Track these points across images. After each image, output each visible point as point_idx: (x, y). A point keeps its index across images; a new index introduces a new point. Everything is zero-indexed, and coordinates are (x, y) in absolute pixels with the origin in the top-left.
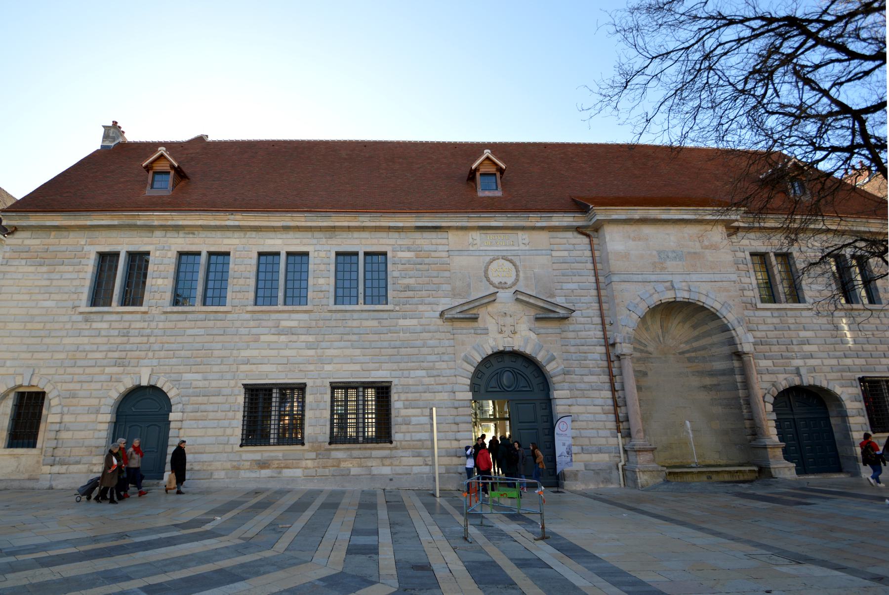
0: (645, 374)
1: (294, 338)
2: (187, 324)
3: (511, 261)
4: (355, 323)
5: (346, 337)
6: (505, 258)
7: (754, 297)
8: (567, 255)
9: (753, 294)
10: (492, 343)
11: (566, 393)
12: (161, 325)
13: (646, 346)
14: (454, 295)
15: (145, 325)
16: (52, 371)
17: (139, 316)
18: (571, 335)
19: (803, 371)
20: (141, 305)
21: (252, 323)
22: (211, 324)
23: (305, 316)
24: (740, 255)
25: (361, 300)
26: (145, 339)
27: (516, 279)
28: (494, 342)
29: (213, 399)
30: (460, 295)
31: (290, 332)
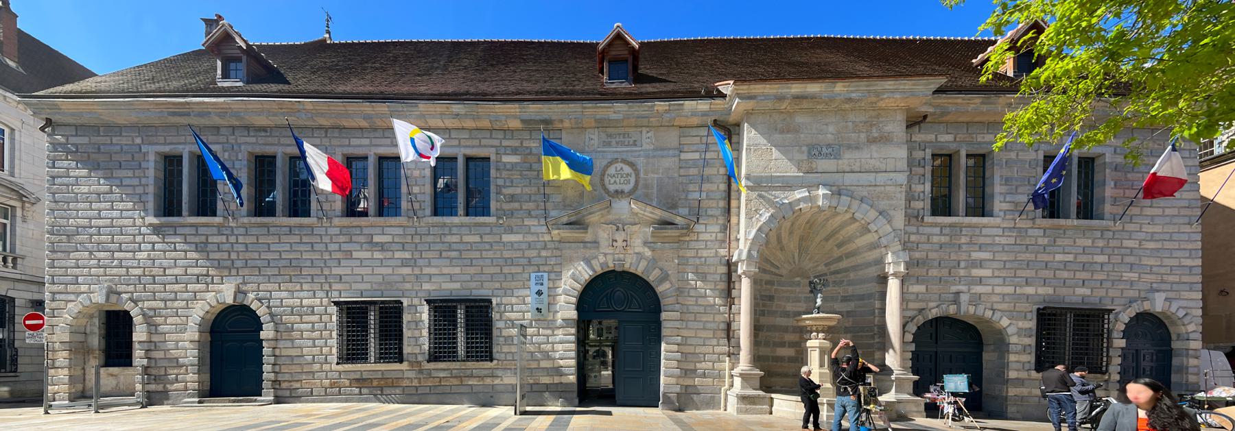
0: (771, 298)
1: (389, 254)
2: (270, 240)
3: (632, 165)
4: (455, 239)
5: (444, 254)
6: (624, 161)
7: (923, 209)
8: (698, 157)
9: (923, 205)
10: (602, 259)
11: (676, 315)
12: (241, 239)
13: (778, 268)
14: (565, 206)
15: (224, 239)
16: (131, 288)
17: (215, 230)
18: (692, 253)
19: (964, 298)
20: (214, 214)
21: (342, 239)
22: (297, 239)
23: (400, 230)
24: (918, 154)
25: (461, 210)
26: (225, 255)
28: (606, 260)
29: (305, 318)
30: (571, 206)
31: (382, 247)
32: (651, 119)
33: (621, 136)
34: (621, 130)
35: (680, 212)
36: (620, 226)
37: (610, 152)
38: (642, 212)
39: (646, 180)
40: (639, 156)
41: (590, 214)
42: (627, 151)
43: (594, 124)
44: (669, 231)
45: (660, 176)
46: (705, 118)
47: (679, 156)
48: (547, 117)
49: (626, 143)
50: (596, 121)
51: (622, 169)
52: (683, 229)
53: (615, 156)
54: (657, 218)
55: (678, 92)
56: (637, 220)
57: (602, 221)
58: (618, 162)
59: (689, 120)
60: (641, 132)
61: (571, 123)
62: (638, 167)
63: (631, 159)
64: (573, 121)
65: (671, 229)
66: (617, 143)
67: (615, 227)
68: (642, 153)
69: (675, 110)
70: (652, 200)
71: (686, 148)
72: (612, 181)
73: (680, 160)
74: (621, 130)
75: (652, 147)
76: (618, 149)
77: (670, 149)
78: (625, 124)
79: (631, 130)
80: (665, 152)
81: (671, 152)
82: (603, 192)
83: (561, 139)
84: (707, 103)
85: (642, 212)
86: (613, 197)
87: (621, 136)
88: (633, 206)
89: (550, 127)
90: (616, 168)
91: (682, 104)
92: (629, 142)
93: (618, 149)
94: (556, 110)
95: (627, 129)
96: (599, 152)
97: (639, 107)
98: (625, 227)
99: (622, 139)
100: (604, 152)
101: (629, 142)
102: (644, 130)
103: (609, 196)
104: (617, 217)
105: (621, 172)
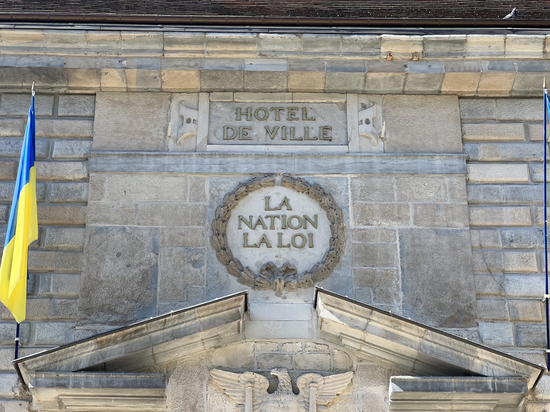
8: (526, 179)
27: (328, 255)
30: (111, 311)
32: (372, 76)
33: (284, 115)
34: (279, 100)
35: (486, 335)
36: (283, 376)
37: (247, 155)
38: (358, 334)
39: (363, 236)
40: (340, 169)
41: (177, 336)
42: (303, 155)
43: (195, 83)
44: (456, 396)
45: (411, 225)
46: (532, 77)
47: (466, 172)
48: (54, 62)
49: (299, 133)
50: (202, 73)
51: (285, 202)
52: (501, 389)
53: (264, 168)
54: (412, 352)
55: (448, 13)
56: (339, 359)
57: (219, 357)
58: (273, 183)
59: (485, 81)
60: (344, 107)
61: (126, 80)
62: (339, 199)
63: (320, 178)
64: (133, 73)
65: (461, 389)
66: (271, 132)
67: (263, 382)
68: (349, 160)
69: (442, 55)
70: (388, 297)
71: (483, 153)
72: (254, 237)
73: (467, 181)
74: (279, 100)
75: (380, 146)
76: (272, 149)
77: (432, 153)
78: (295, 81)
79: (312, 100)
80: (421, 163)
81: (438, 162)
82: (221, 269)
83: (91, 118)
84: (534, 41)
85: (358, 334)
86: (256, 286)
87: (284, 115)
88: (324, 312)
89: (60, 86)
90: (267, 199)
91: (462, 42)
92: (307, 130)
93: (272, 149)
94: (82, 45)
95: (300, 99)
96: (212, 154)
97: (335, 44)
98: (301, 382)
99: (284, 121)
100: (225, 155)
101: (307, 130)
102: (353, 102)
103: (242, 281)
104: (271, 347)
105: (284, 211)
